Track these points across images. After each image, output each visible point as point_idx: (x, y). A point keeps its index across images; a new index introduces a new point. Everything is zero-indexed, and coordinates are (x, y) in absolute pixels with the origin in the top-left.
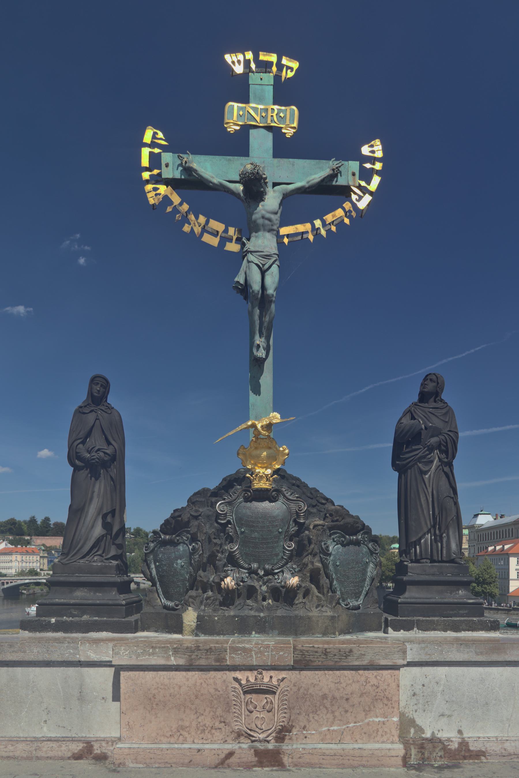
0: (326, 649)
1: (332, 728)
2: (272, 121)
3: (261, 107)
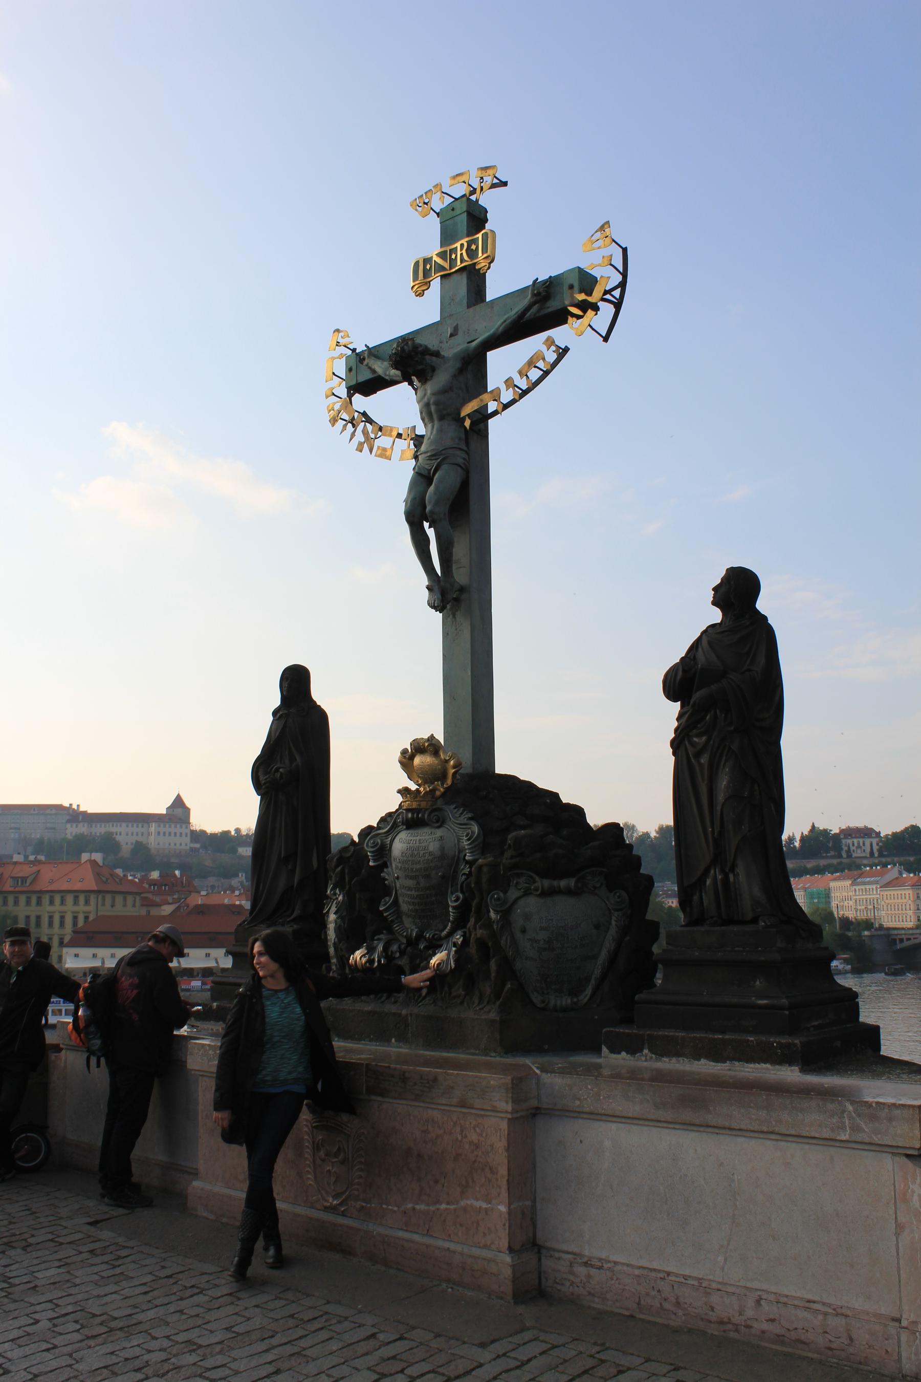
0: (404, 1072)
1: (418, 1207)
2: (462, 260)
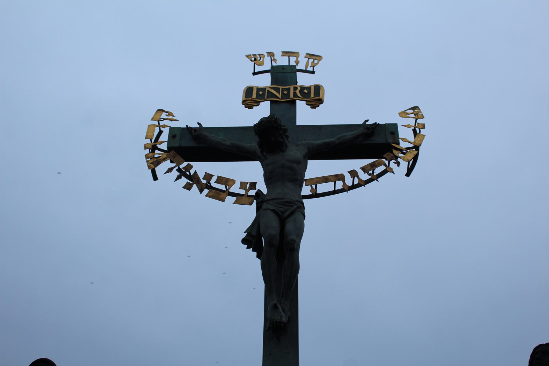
2: (295, 95)
3: (281, 87)
